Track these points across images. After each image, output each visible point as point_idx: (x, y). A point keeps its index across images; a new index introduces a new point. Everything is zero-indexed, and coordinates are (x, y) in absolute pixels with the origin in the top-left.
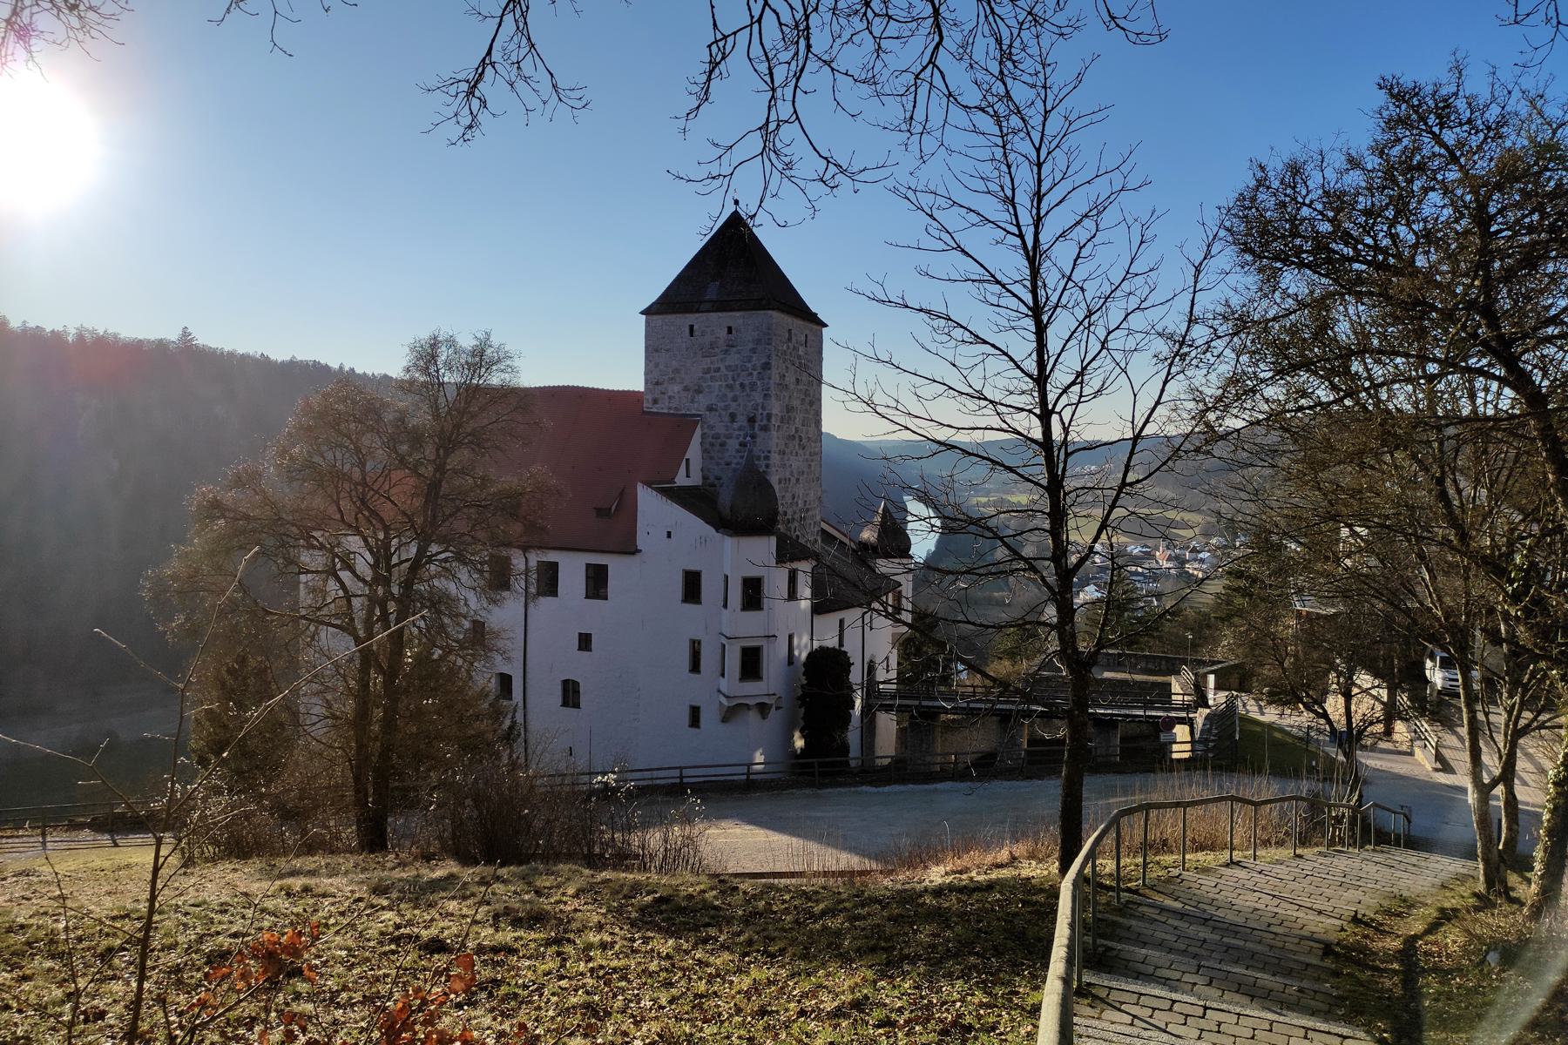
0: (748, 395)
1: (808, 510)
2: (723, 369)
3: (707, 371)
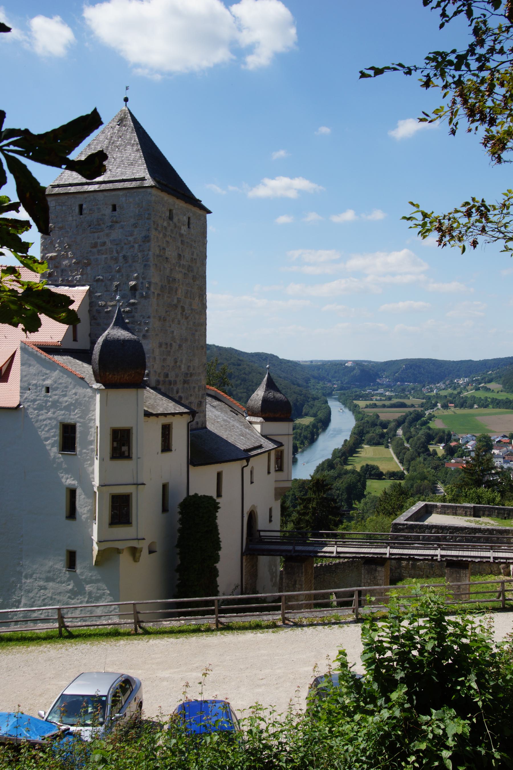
0: (130, 266)
1: (191, 375)
2: (109, 245)
3: (95, 245)
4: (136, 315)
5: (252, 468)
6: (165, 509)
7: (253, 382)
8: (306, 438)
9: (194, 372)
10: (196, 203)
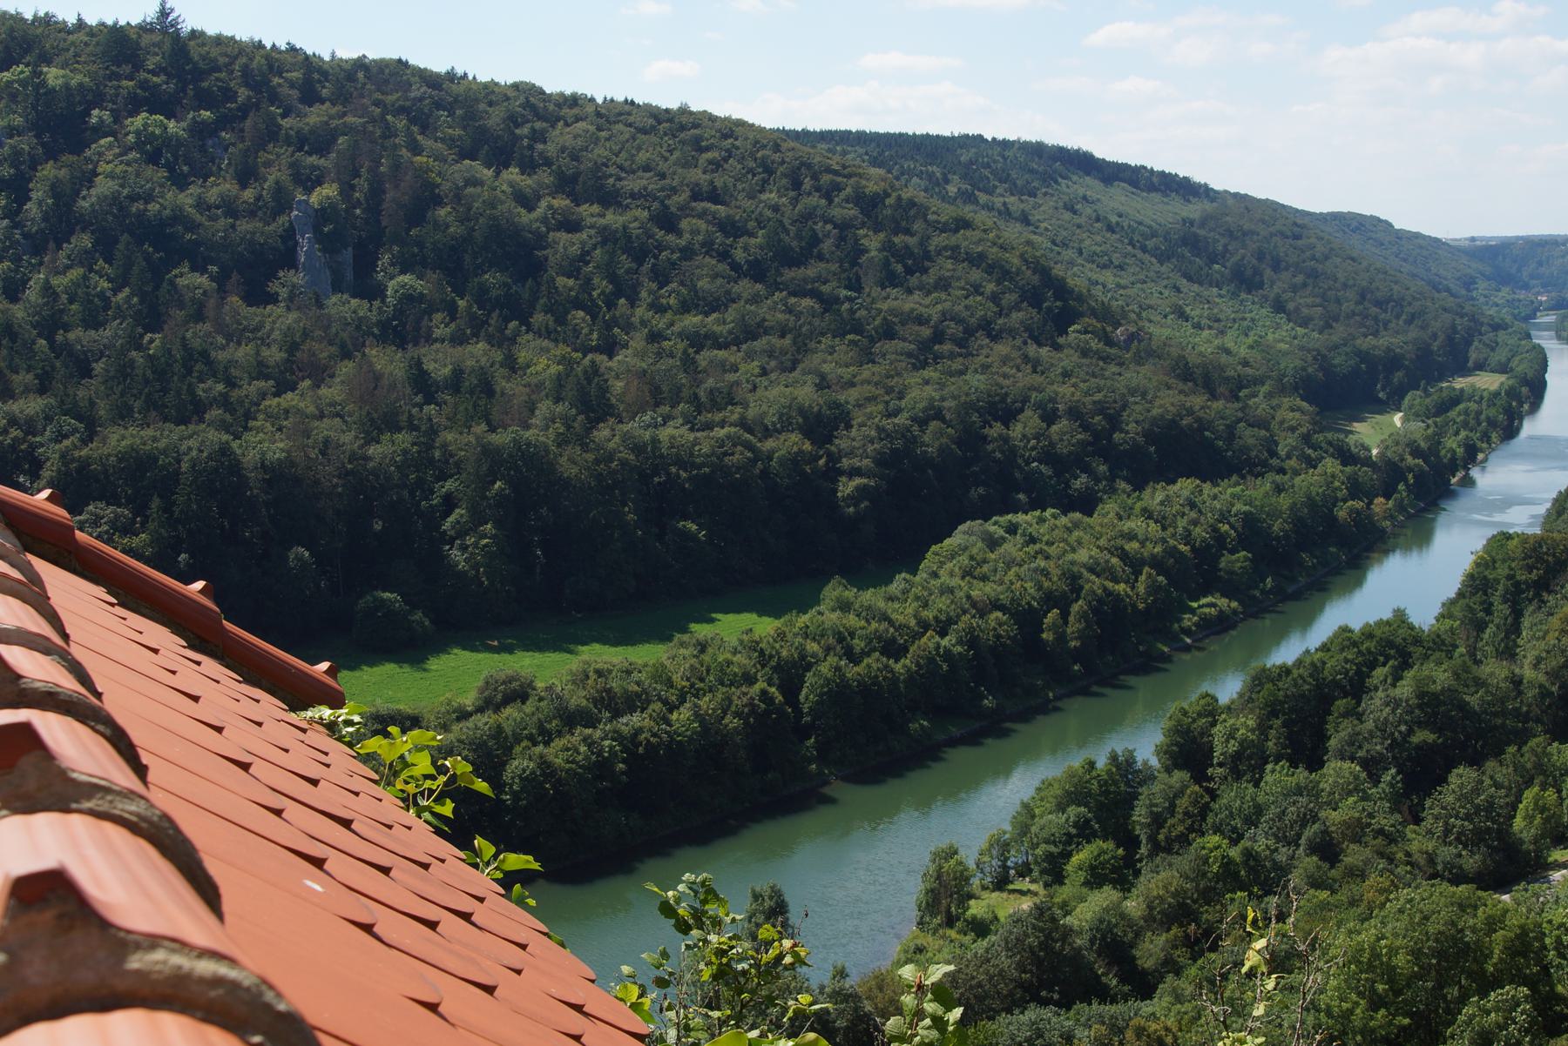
7: (1336, 280)
8: (1492, 423)
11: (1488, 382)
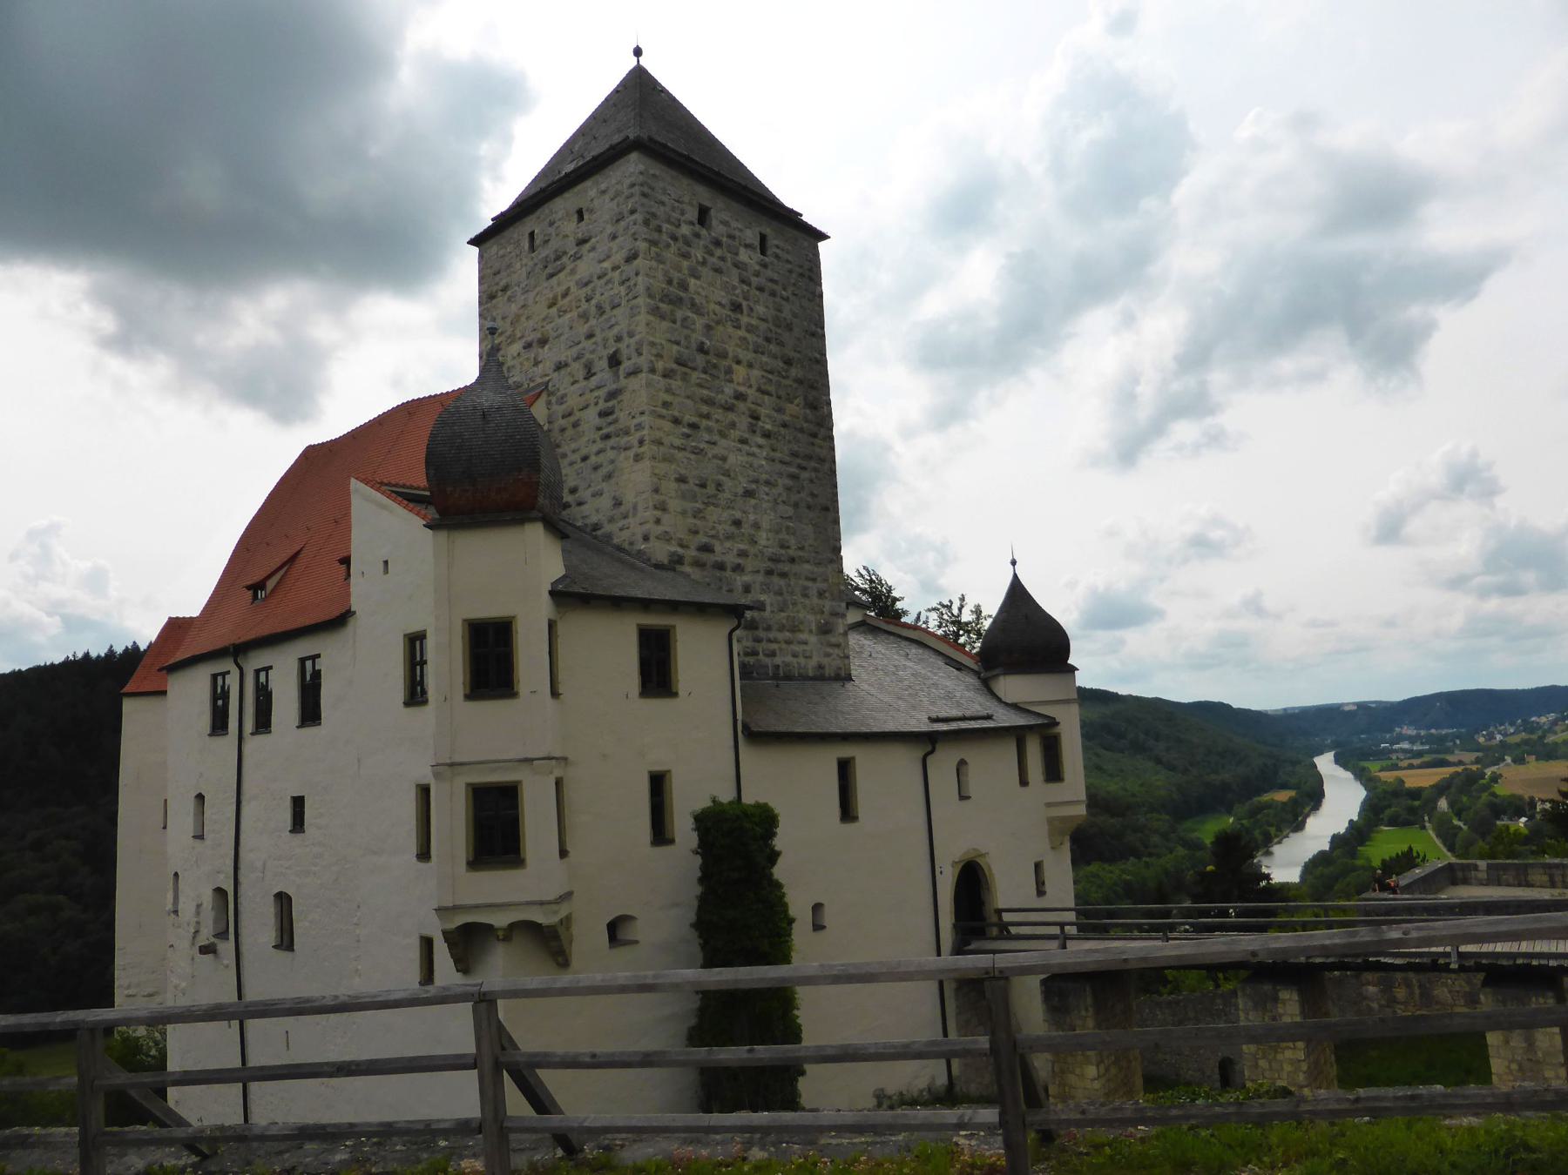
2: (573, 289)
4: (622, 415)
5: (962, 763)
6: (661, 833)
9: (801, 553)
10: (789, 220)
11: (1283, 796)
